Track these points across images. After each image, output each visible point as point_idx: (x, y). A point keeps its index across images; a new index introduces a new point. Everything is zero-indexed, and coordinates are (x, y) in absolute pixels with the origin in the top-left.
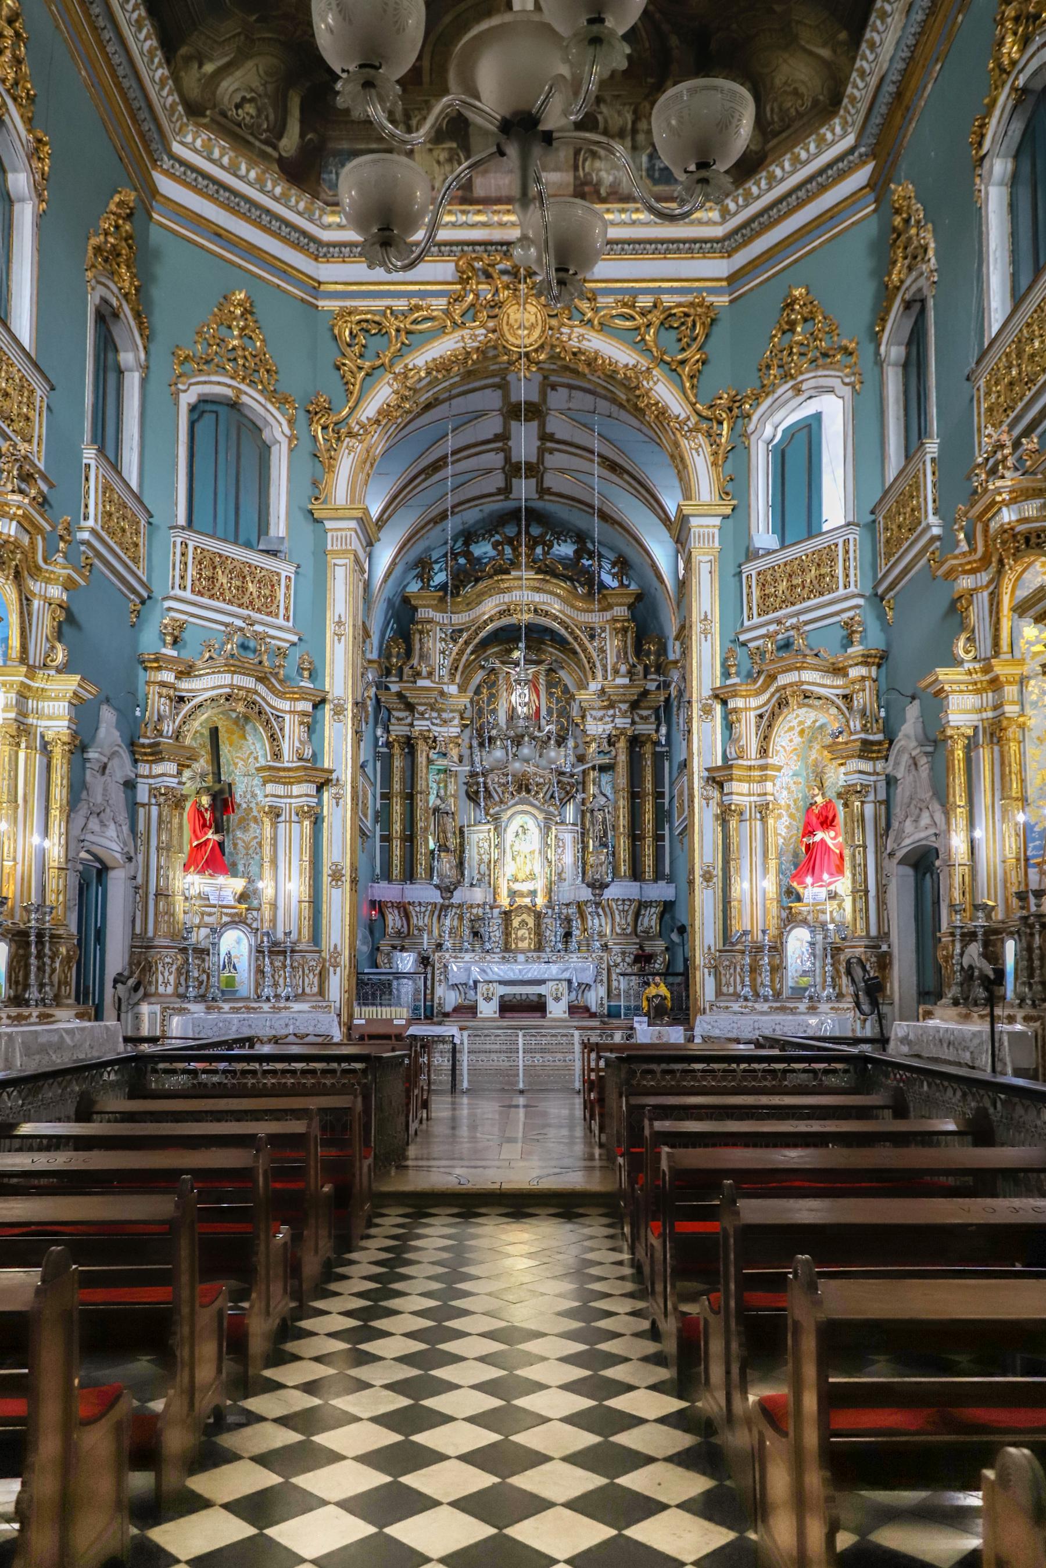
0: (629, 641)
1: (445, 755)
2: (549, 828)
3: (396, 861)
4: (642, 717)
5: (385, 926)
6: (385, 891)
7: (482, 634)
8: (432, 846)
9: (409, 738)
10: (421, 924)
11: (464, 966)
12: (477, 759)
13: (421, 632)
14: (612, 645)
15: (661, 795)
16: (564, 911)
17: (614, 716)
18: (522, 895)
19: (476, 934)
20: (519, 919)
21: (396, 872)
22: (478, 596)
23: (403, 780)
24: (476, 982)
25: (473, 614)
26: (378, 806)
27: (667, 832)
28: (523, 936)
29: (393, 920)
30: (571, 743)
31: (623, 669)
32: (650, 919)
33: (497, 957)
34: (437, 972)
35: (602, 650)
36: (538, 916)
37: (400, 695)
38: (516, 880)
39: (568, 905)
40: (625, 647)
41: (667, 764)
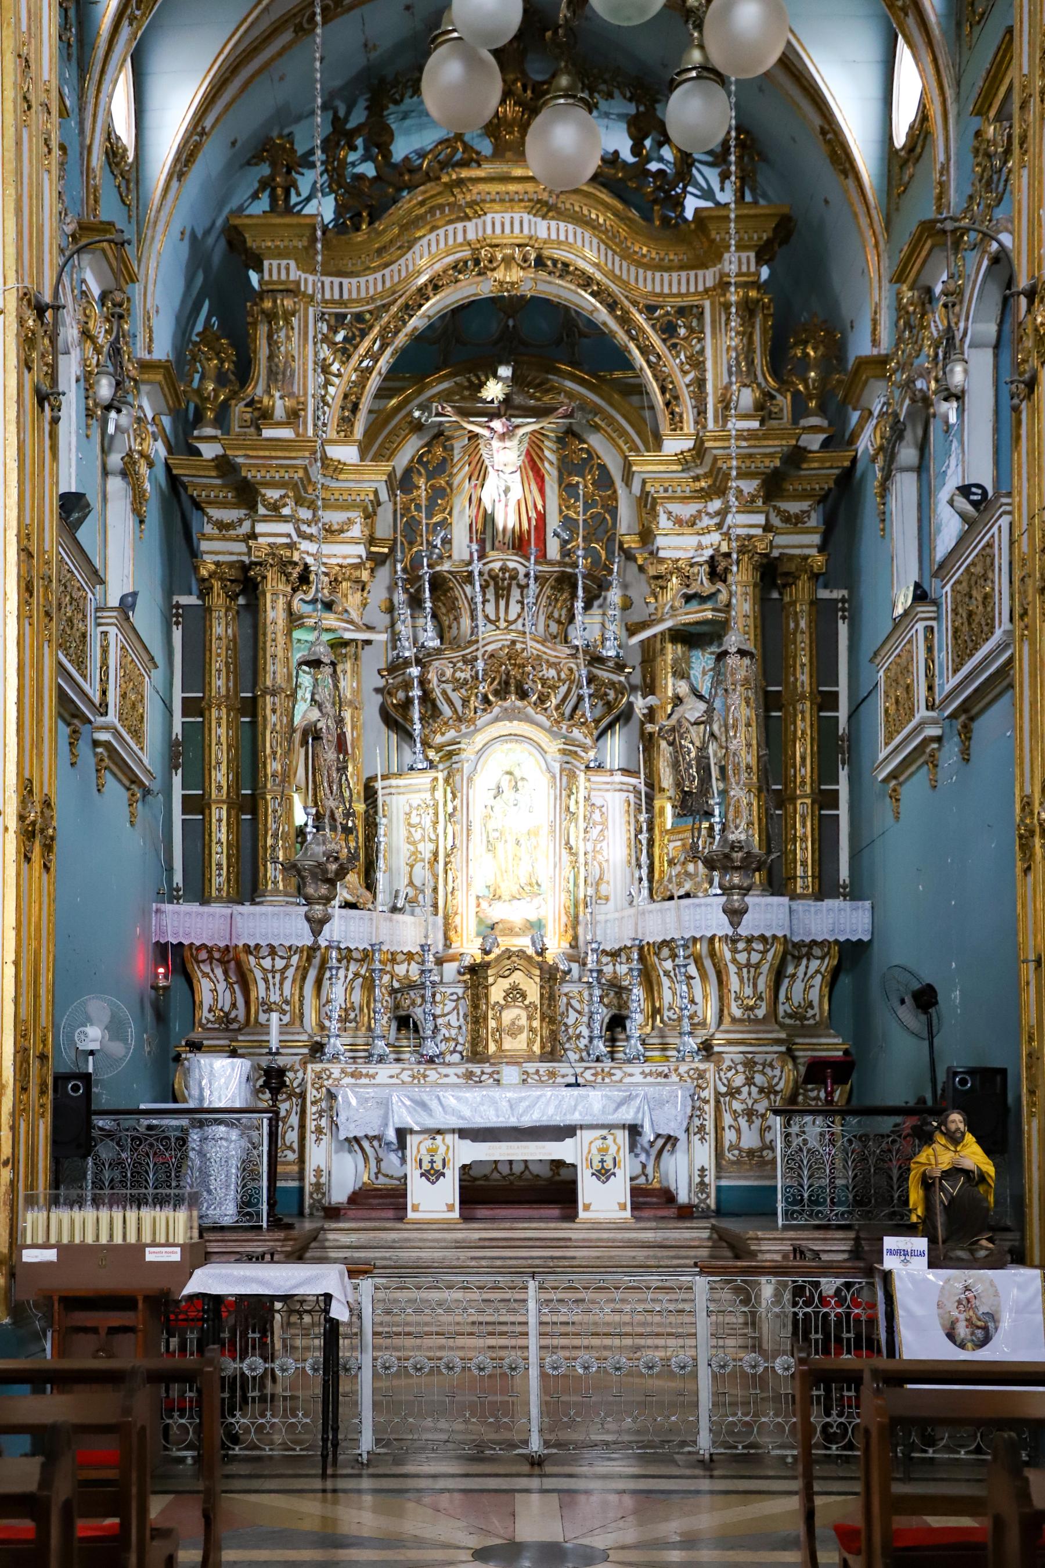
0: (757, 338)
1: (328, 606)
2: (572, 776)
3: (219, 855)
4: (787, 518)
5: (194, 1005)
6: (192, 923)
7: (416, 322)
8: (300, 817)
9: (245, 568)
10: (275, 997)
11: (372, 1096)
12: (404, 629)
13: (271, 317)
14: (720, 348)
15: (830, 701)
16: (608, 969)
17: (723, 513)
18: (511, 931)
19: (404, 1022)
20: (504, 984)
21: (219, 880)
22: (404, 228)
23: (234, 669)
24: (402, 1134)
25: (391, 275)
26: (177, 729)
27: (843, 788)
28: (516, 1027)
29: (212, 990)
30: (614, 595)
31: (747, 398)
32: (807, 986)
33: (453, 1074)
34: (311, 1109)
35: (697, 363)
36: (551, 976)
37: (224, 466)
38: (496, 897)
39: (615, 954)
40: (749, 350)
41: (843, 629)
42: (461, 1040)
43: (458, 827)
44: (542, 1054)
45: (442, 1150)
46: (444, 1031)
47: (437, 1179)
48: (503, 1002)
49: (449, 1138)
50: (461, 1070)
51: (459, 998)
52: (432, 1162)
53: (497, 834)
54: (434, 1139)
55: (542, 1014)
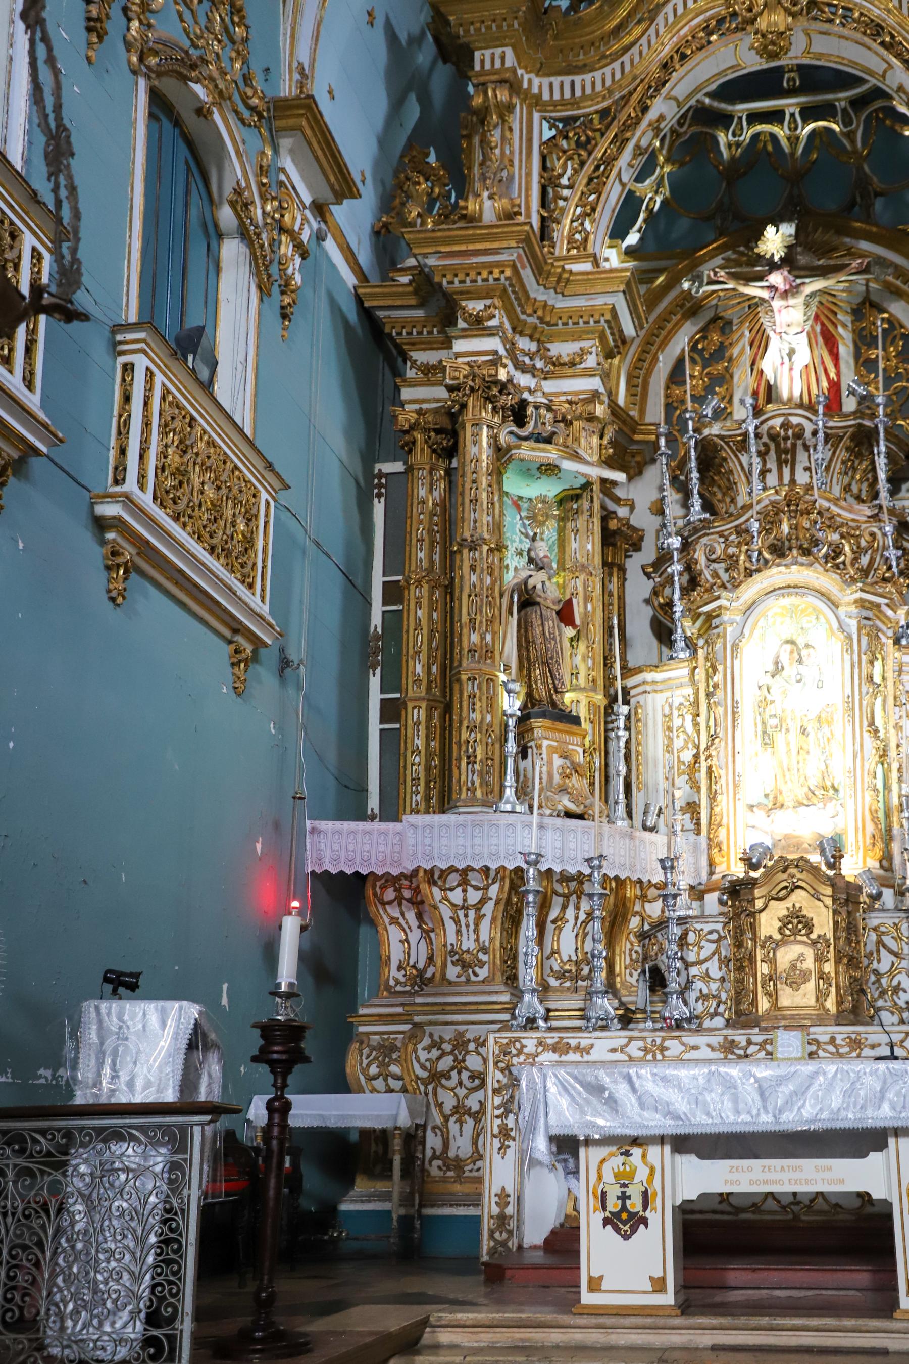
42: (724, 996)
43: (720, 710)
44: (840, 1013)
45: (642, 1174)
46: (699, 985)
47: (634, 1230)
48: (777, 936)
49: (654, 1152)
50: (716, 1040)
51: (720, 938)
52: (624, 1197)
53: (773, 722)
54: (627, 1154)
55: (838, 952)
